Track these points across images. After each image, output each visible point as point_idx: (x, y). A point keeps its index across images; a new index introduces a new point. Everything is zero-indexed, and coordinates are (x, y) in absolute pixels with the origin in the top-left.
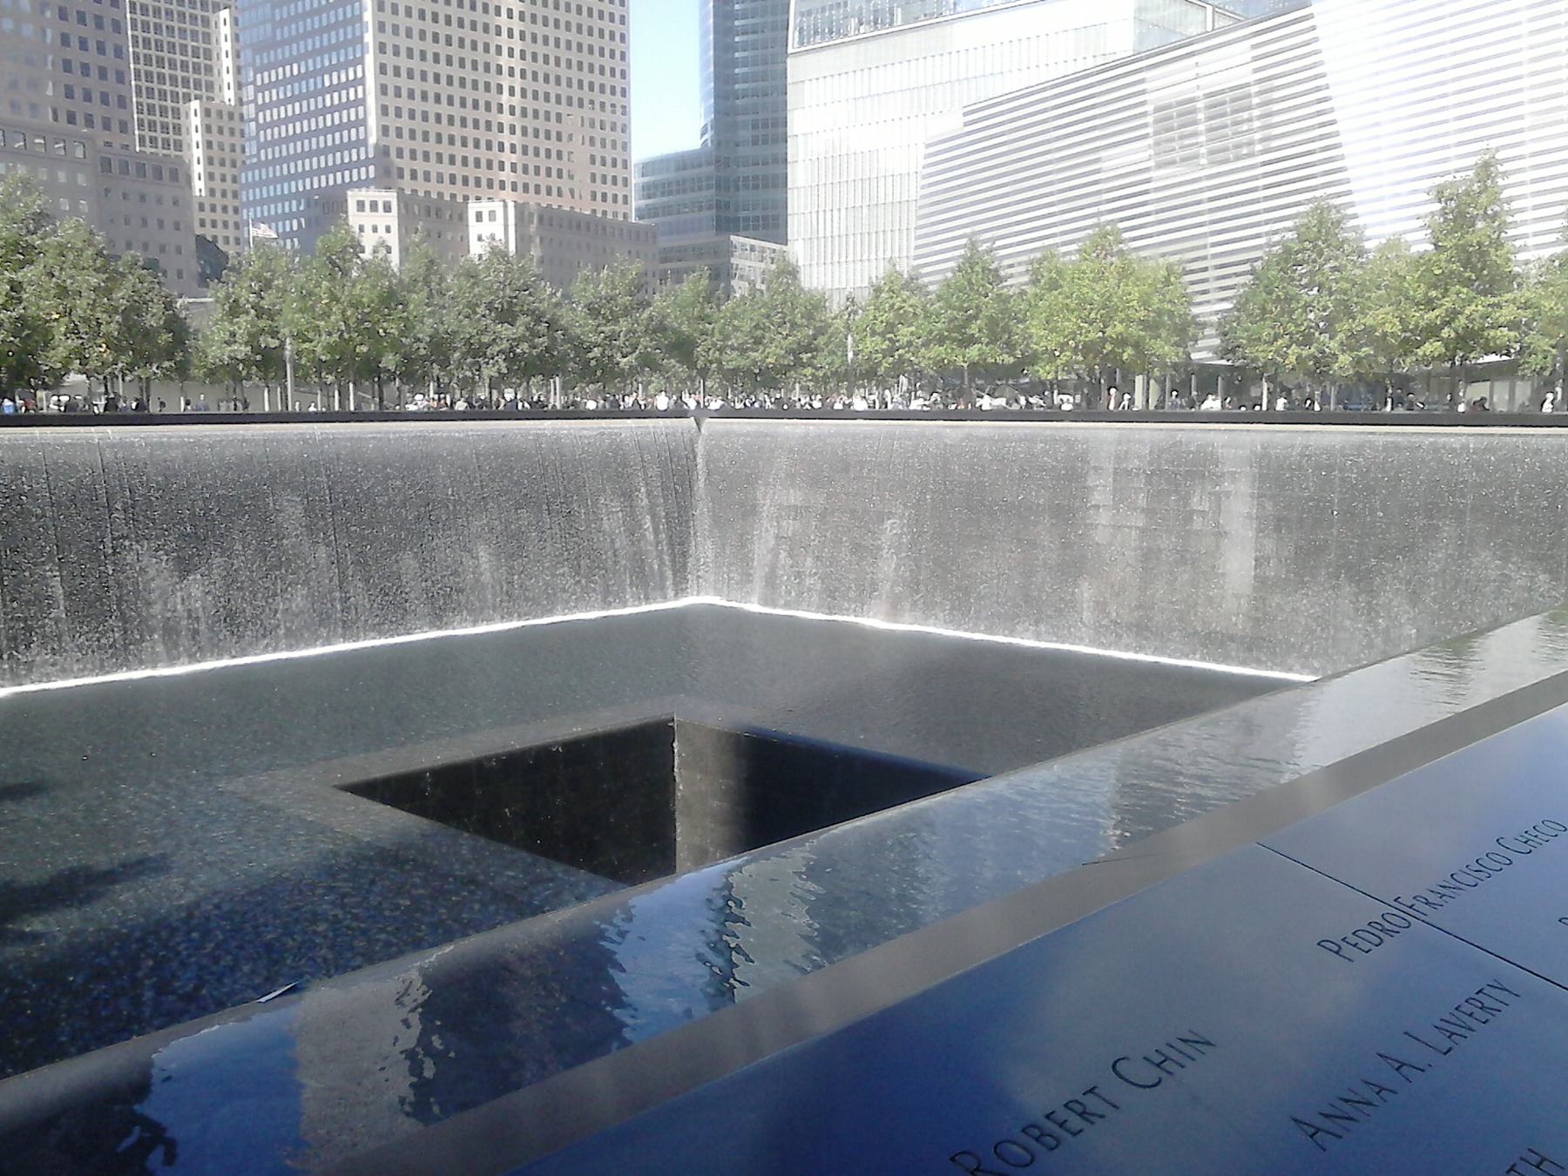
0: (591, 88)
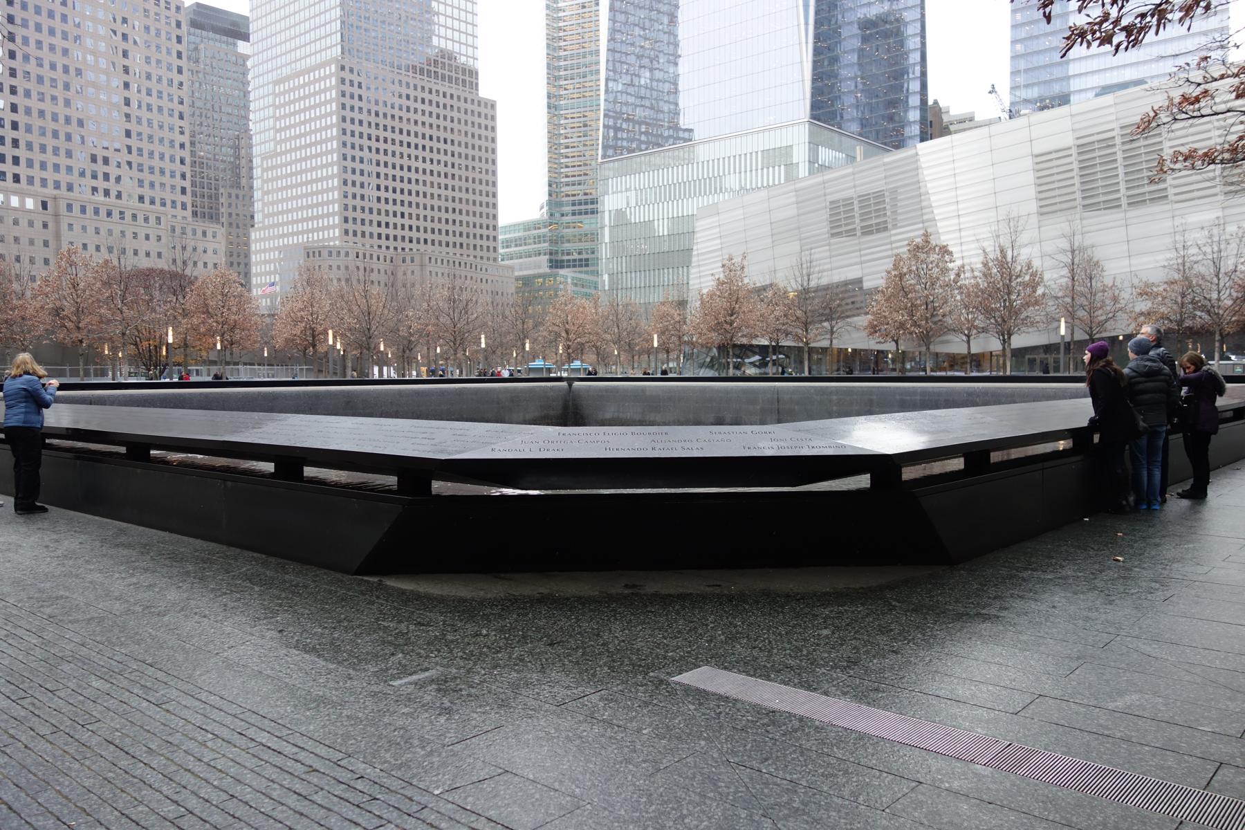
0: (474, 182)
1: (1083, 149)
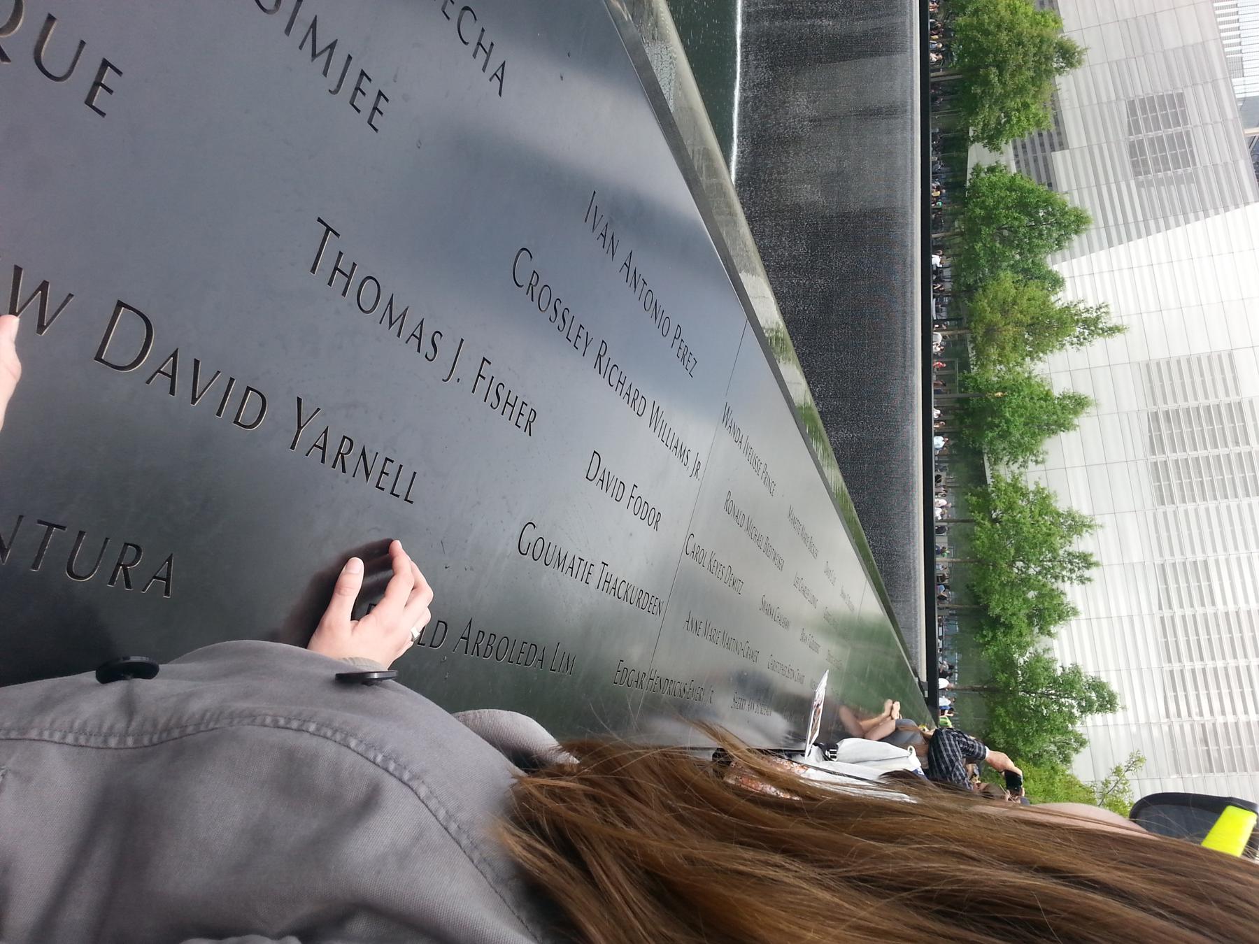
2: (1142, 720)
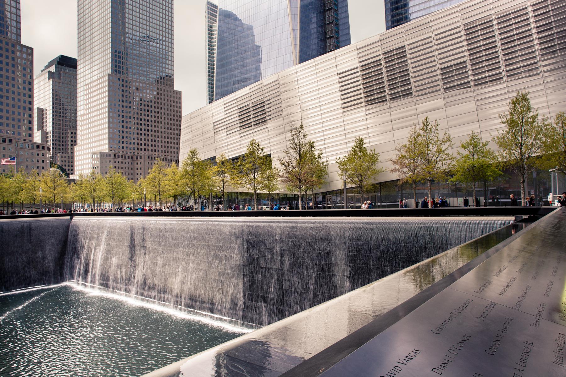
1: (364, 68)
2: (542, 87)
